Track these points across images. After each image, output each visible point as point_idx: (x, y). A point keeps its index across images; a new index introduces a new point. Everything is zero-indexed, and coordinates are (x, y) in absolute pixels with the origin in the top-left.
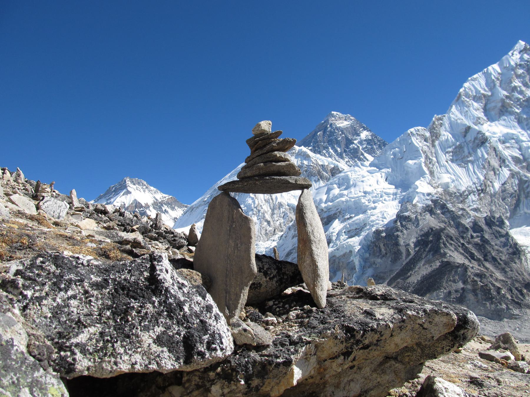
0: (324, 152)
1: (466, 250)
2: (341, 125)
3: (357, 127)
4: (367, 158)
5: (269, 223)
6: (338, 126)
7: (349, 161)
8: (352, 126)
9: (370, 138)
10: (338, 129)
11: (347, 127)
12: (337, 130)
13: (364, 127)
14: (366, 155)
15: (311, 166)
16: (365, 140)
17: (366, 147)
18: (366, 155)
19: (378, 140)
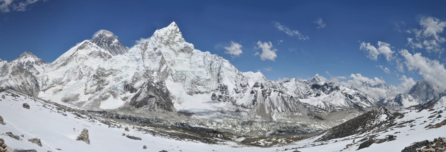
1: (155, 91)
5: (82, 73)
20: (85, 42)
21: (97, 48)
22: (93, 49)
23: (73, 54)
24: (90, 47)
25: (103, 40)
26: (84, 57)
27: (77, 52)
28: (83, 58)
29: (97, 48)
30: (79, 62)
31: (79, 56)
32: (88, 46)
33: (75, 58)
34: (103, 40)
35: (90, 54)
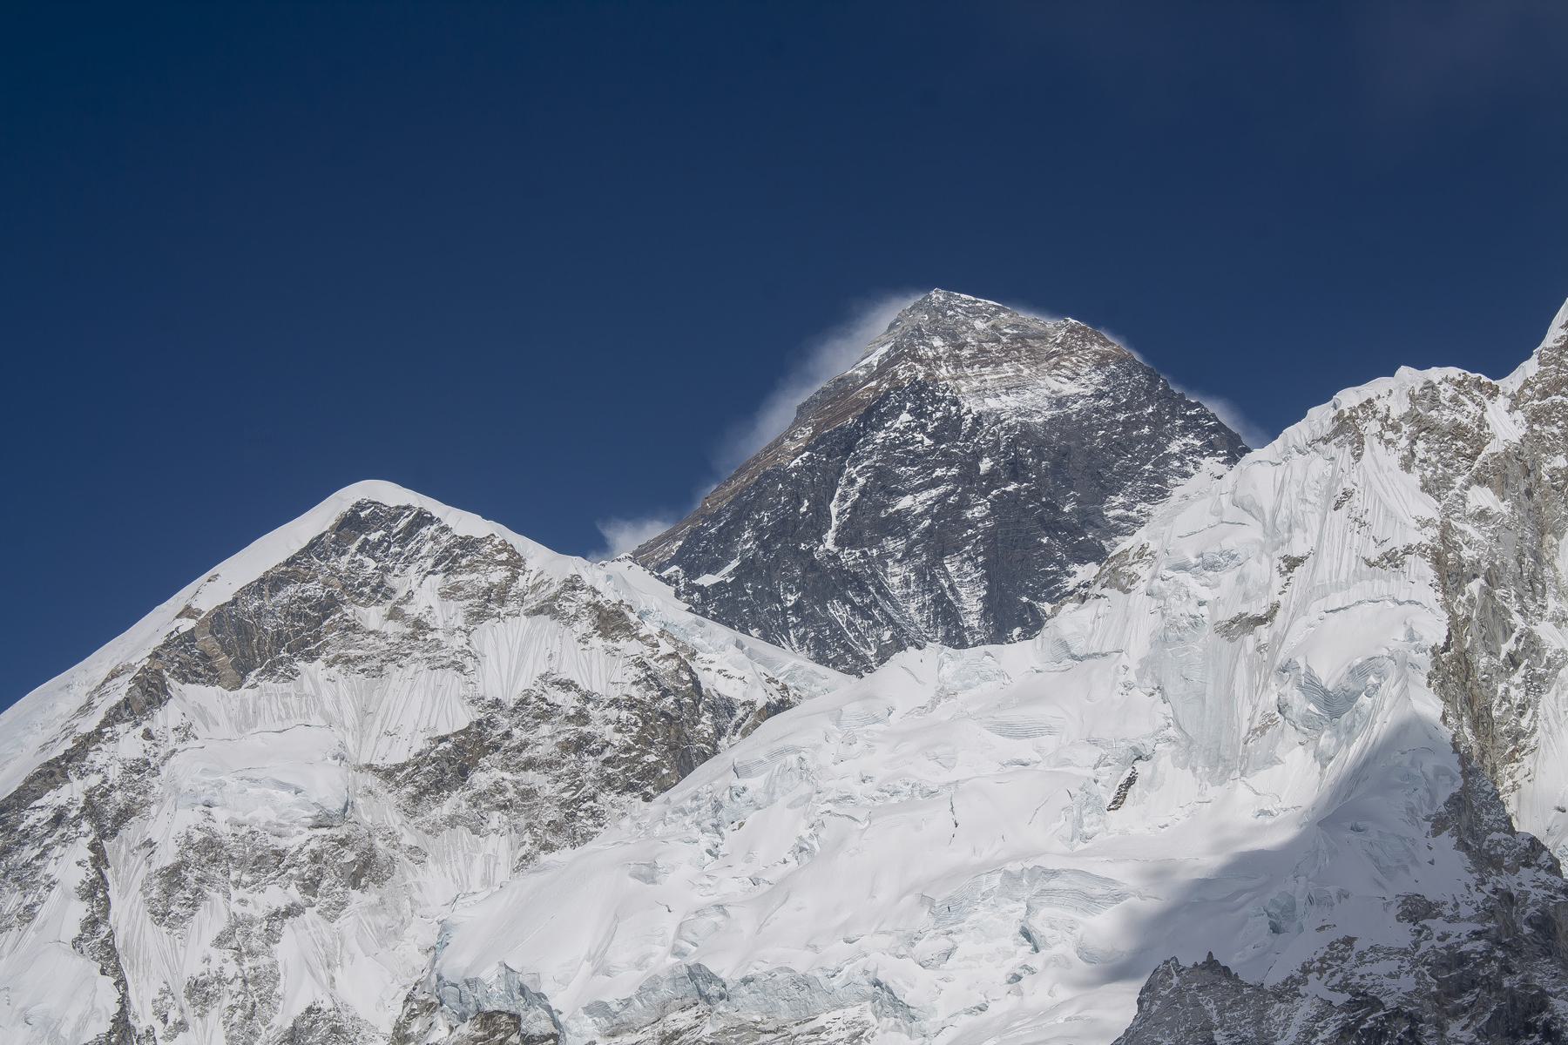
0: (839, 612)
15: (632, 704)
20: (351, 523)
21: (611, 621)
22: (517, 656)
23: (51, 774)
24: (446, 615)
25: (885, 484)
26: (299, 840)
27: (128, 744)
28: (266, 862)
29: (611, 621)
30: (165, 957)
31: (166, 828)
32: (423, 592)
33: (68, 865)
34: (885, 484)
35: (449, 765)
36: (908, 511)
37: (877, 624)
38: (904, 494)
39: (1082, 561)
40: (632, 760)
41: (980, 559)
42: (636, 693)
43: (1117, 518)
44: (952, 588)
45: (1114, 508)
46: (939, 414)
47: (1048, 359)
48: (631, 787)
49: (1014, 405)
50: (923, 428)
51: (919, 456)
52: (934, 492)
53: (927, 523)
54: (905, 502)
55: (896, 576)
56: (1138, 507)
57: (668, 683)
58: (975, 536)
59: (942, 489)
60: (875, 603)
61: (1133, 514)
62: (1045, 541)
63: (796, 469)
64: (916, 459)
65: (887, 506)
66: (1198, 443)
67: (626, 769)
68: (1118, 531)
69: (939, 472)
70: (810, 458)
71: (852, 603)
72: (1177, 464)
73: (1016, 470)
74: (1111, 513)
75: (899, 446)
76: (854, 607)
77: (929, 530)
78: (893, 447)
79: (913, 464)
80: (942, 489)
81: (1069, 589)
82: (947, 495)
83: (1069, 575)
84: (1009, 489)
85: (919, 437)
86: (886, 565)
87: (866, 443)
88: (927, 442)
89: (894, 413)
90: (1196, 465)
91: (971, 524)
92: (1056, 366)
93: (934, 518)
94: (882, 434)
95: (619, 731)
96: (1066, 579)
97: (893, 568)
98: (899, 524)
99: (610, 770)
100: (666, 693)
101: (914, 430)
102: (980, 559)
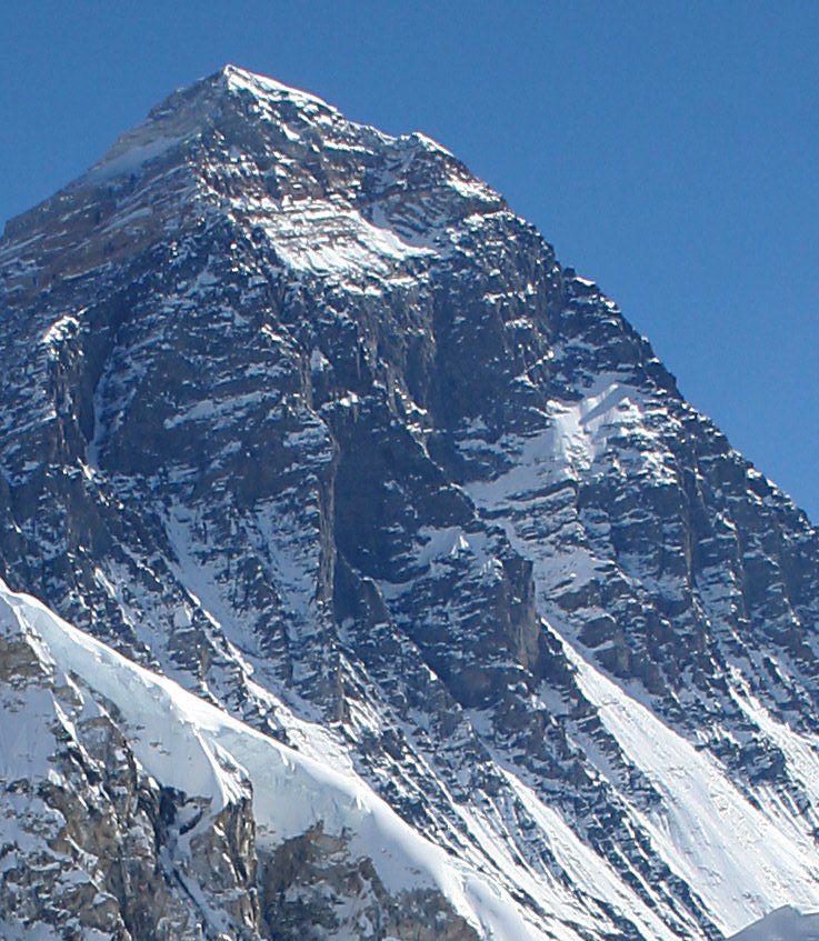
2: (334, 260)
3: (514, 304)
4: (611, 721)
6: (297, 262)
7: (389, 743)
8: (453, 294)
9: (657, 466)
10: (297, 302)
11: (393, 298)
12: (287, 314)
13: (587, 320)
14: (594, 684)
15: (47, 793)
16: (594, 495)
17: (601, 593)
18: (594, 684)
19: (748, 517)
36: (206, 423)
37: (168, 600)
38: (202, 394)
39: (439, 524)
40: (49, 875)
41: (310, 509)
42: (56, 778)
43: (469, 451)
44: (264, 549)
45: (470, 437)
46: (263, 280)
47: (384, 196)
48: (50, 917)
49: (343, 264)
50: (233, 299)
51: (227, 340)
52: (247, 398)
53: (236, 445)
54: (205, 408)
55: (179, 522)
56: (504, 439)
57: (95, 764)
58: (303, 473)
59: (255, 397)
60: (159, 567)
61: (496, 448)
62: (389, 485)
63: (57, 345)
64: (223, 344)
65: (176, 412)
66: (593, 348)
67: (38, 889)
68: (481, 475)
69: (253, 370)
70: (70, 326)
71: (123, 559)
72: (560, 377)
73: (350, 374)
74: (464, 445)
75: (197, 322)
76: (134, 570)
77: (235, 460)
78: (188, 320)
79: (216, 351)
80: (255, 397)
81: (420, 562)
82: (268, 404)
83: (423, 541)
84: (345, 402)
85: (228, 311)
86: (168, 503)
87: (147, 310)
88: (239, 320)
89: (190, 268)
90: (589, 382)
91: (295, 454)
92: (398, 208)
93: (243, 437)
94: (174, 298)
95: (29, 829)
96: (417, 546)
97: (179, 509)
98: (195, 445)
99: (12, 886)
100: (93, 778)
101: (219, 300)
102: (310, 509)
